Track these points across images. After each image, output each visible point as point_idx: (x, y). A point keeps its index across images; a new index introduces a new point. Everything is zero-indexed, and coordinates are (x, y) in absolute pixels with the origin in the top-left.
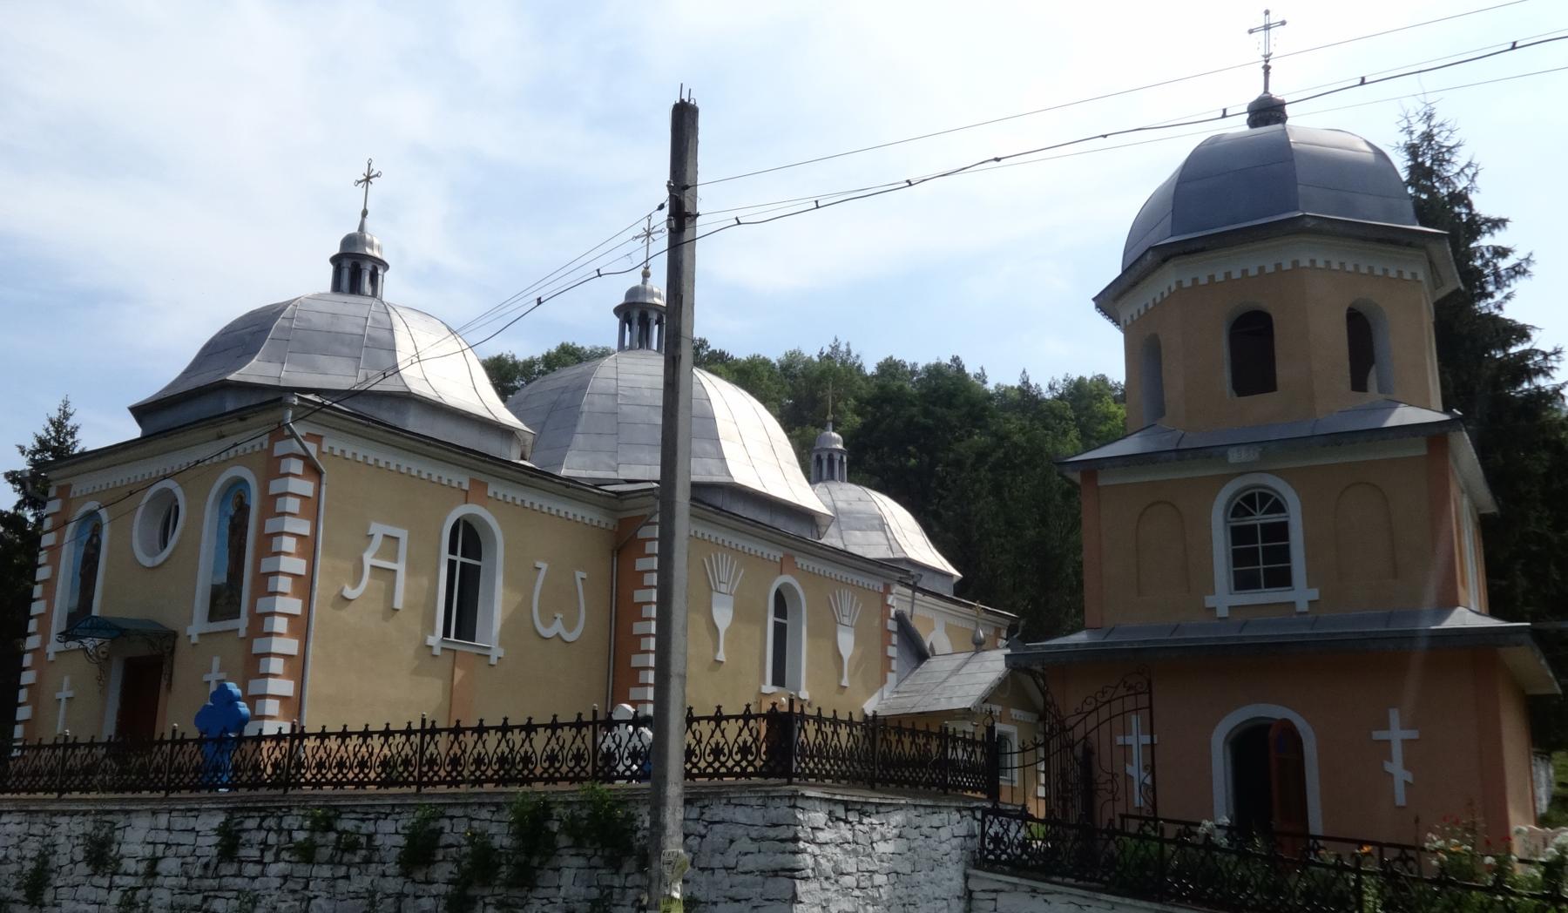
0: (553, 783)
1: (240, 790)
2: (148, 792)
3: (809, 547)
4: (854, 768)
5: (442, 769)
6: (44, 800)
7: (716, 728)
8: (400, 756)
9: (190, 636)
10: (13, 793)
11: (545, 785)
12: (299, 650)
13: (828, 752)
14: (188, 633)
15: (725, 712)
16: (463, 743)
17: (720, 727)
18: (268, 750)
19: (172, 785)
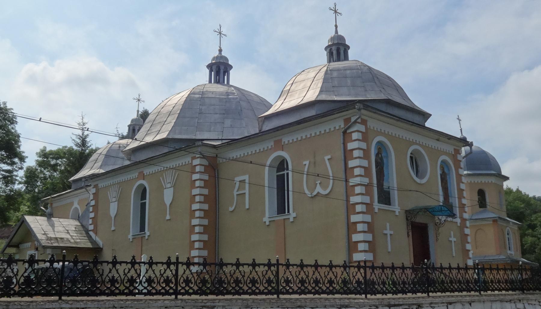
0: (385, 295)
1: (463, 292)
2: (411, 294)
3: (507, 242)
4: (501, 286)
5: (245, 285)
6: (512, 294)
7: (268, 270)
8: (401, 279)
9: (265, 222)
10: (356, 294)
11: (382, 295)
12: (352, 237)
13: (495, 281)
14: (264, 221)
15: (305, 263)
16: (406, 274)
17: (317, 270)
18: (455, 274)
19: (478, 289)
